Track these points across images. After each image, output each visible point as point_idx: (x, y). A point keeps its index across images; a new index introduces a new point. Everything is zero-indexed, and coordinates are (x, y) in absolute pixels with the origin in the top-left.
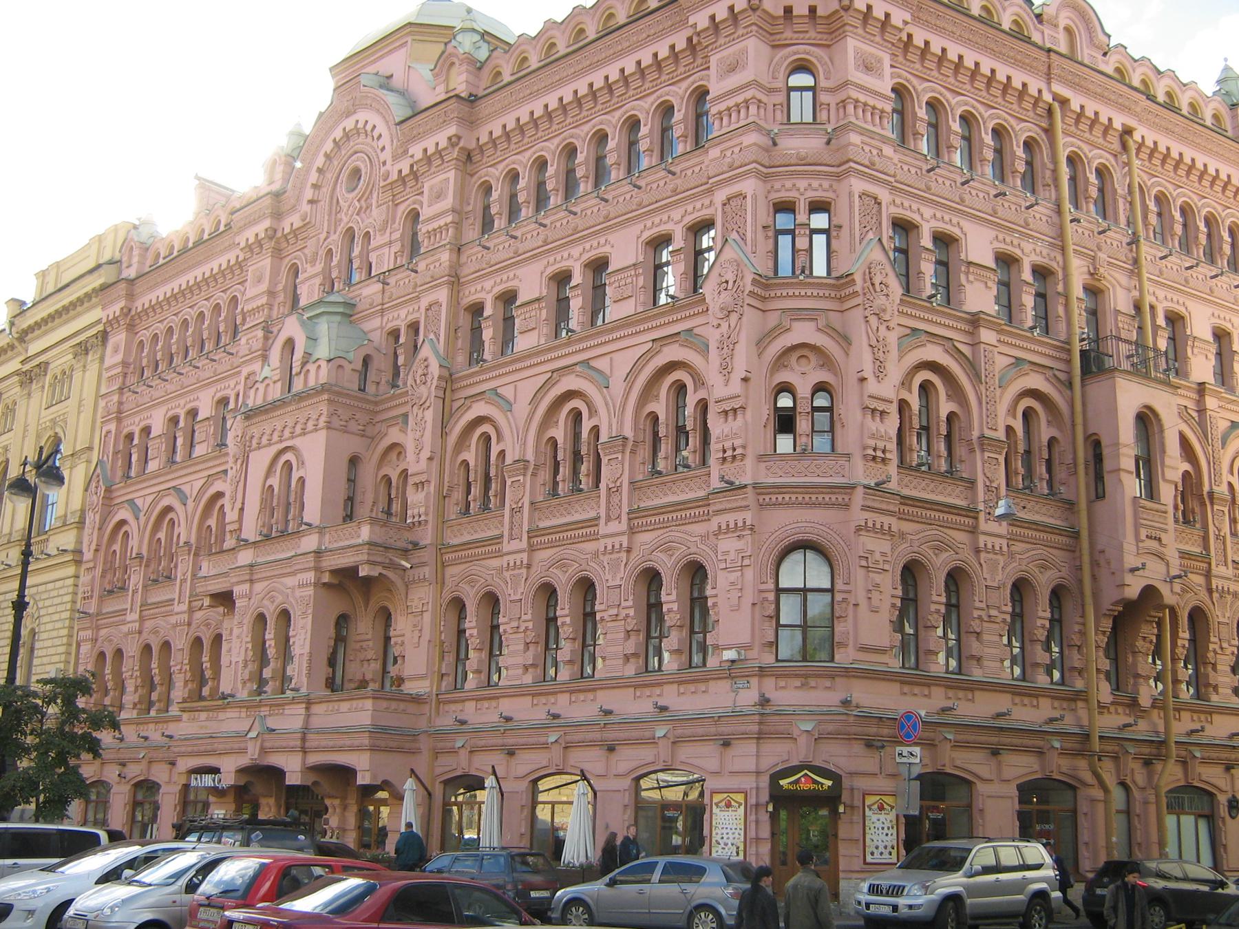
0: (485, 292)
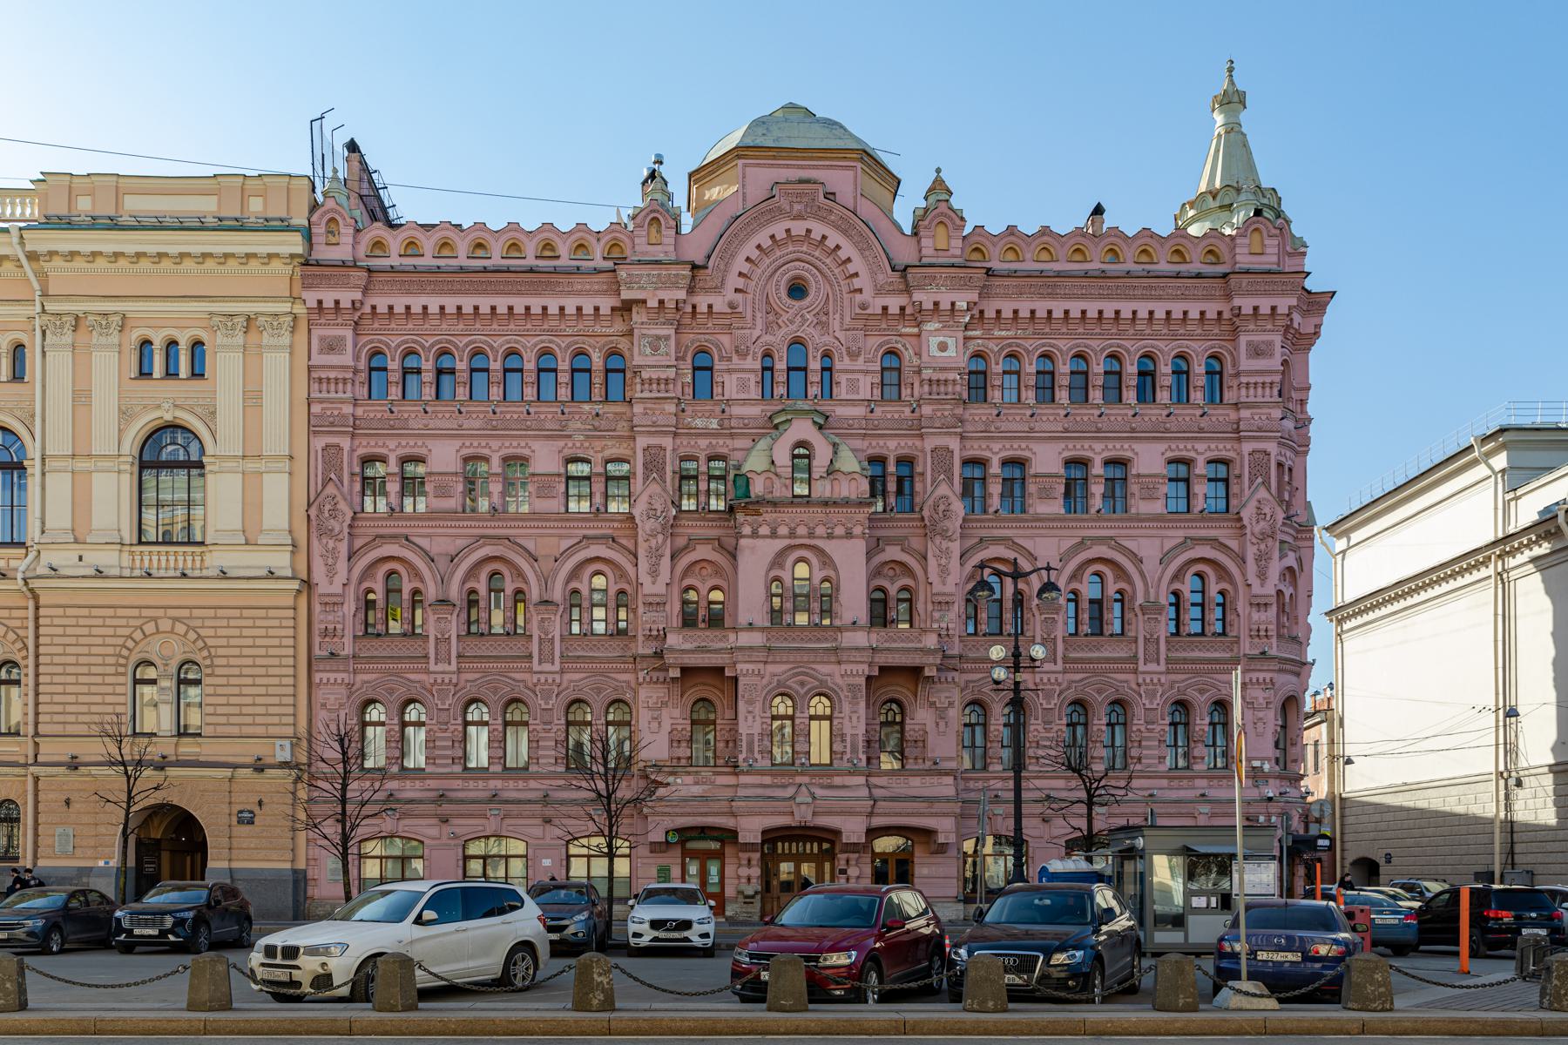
0: (995, 454)
